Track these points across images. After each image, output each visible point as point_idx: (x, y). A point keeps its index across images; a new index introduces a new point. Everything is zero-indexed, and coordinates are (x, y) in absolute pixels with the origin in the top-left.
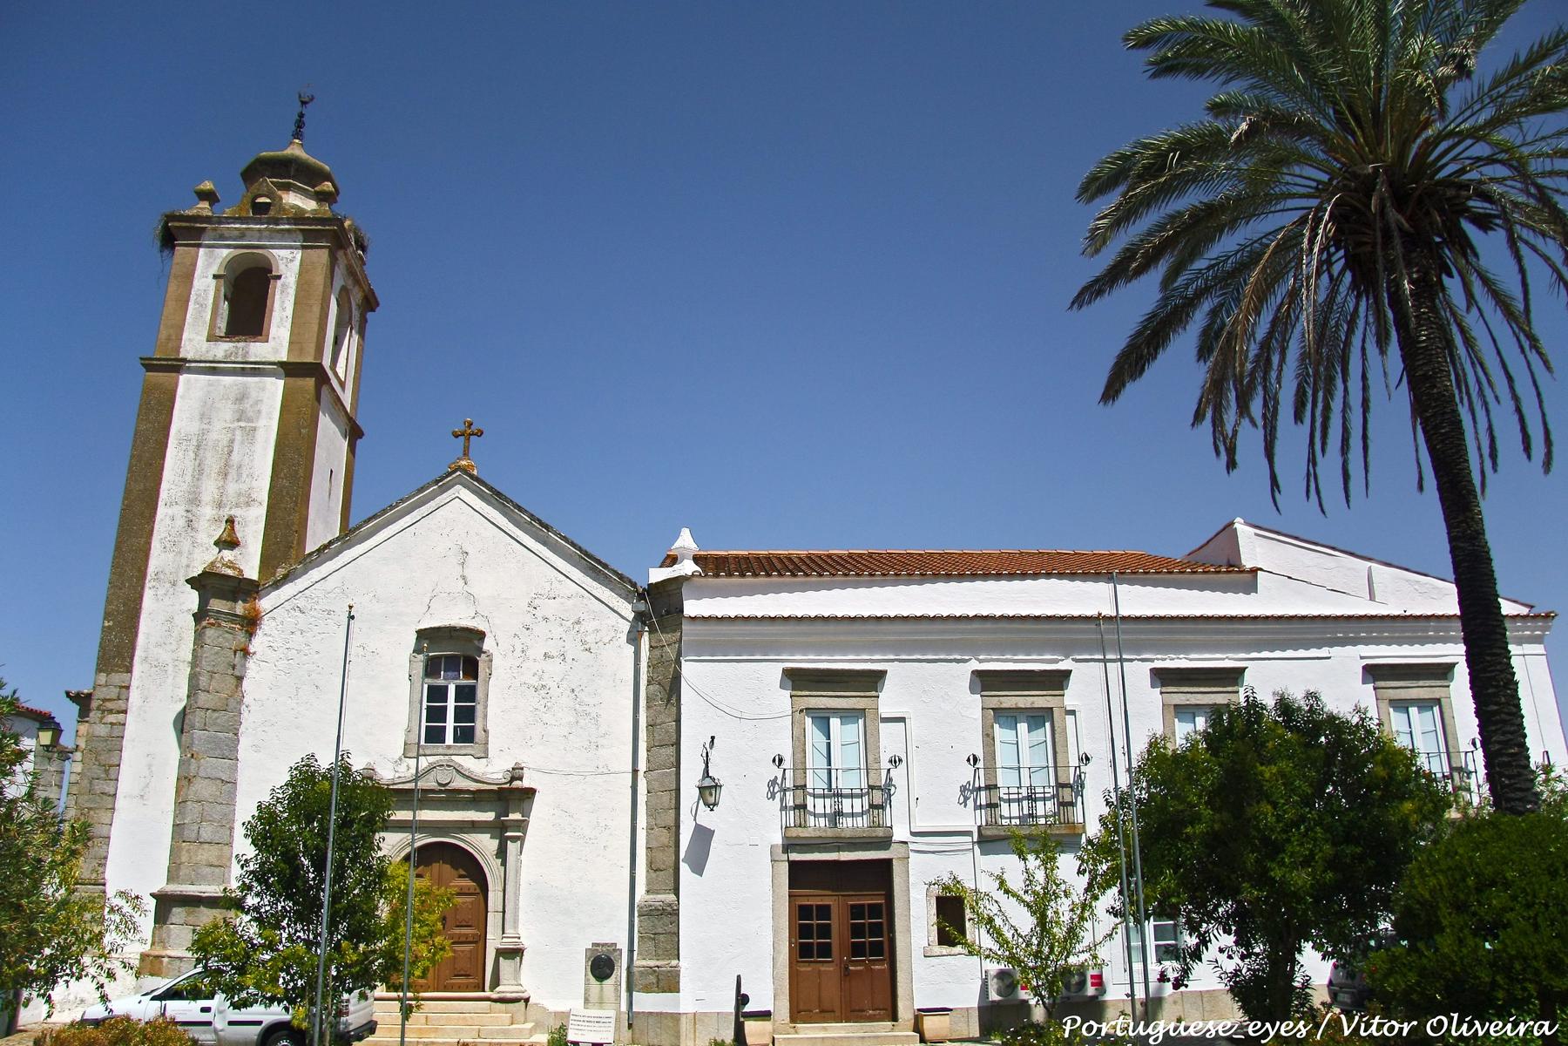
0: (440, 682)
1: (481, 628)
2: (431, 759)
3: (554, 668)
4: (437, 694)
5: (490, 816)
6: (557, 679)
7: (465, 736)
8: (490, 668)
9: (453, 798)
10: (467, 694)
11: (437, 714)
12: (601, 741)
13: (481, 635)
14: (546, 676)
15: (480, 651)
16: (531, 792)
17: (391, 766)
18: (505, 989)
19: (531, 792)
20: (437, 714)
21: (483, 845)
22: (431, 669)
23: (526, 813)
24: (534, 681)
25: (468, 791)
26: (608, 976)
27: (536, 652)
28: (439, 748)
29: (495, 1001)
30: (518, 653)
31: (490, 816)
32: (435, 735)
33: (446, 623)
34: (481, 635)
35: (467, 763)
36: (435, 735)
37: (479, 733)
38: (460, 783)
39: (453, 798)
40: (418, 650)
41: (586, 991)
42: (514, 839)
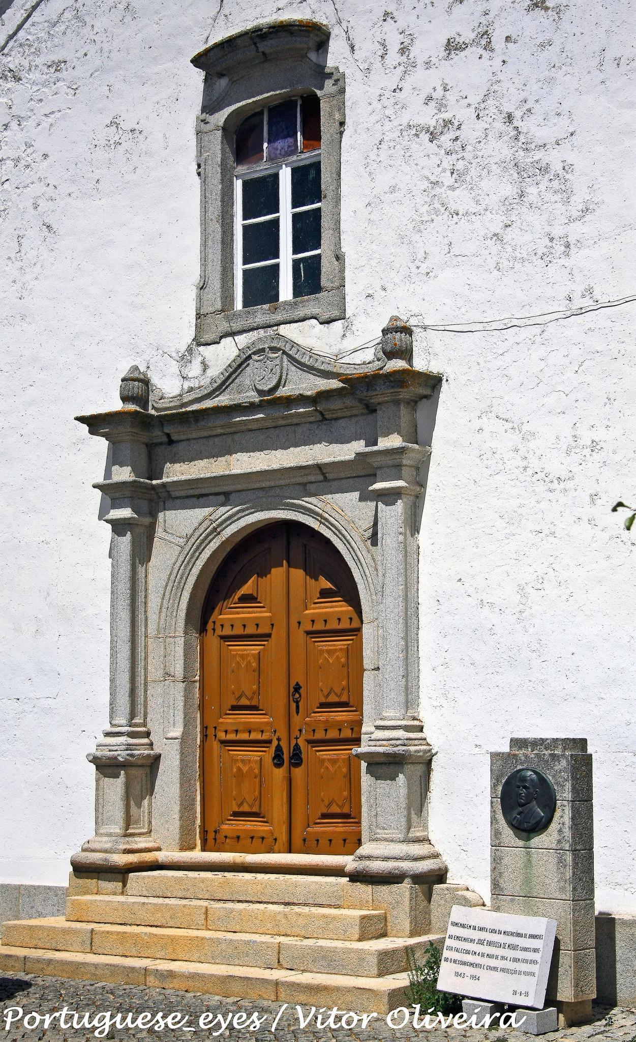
0: (260, 169)
1: (320, 19)
2: (243, 340)
3: (470, 71)
4: (261, 195)
5: (346, 451)
6: (474, 99)
7: (309, 279)
8: (341, 108)
9: (278, 418)
10: (308, 184)
11: (262, 242)
12: (576, 231)
13: (315, 36)
14: (451, 97)
15: (322, 74)
16: (434, 382)
17: (174, 367)
18: (379, 850)
19: (434, 382)
20: (262, 242)
21: (341, 515)
22: (242, 140)
23: (420, 435)
24: (428, 117)
25: (301, 399)
26: (541, 826)
27: (428, 45)
28: (261, 314)
29: (357, 877)
30: (394, 57)
31: (346, 451)
32: (261, 288)
33: (249, 26)
34: (315, 36)
35: (309, 336)
36: (261, 288)
37: (327, 266)
38: (303, 384)
39: (278, 418)
40: (210, 107)
41: (496, 861)
42: (389, 497)
